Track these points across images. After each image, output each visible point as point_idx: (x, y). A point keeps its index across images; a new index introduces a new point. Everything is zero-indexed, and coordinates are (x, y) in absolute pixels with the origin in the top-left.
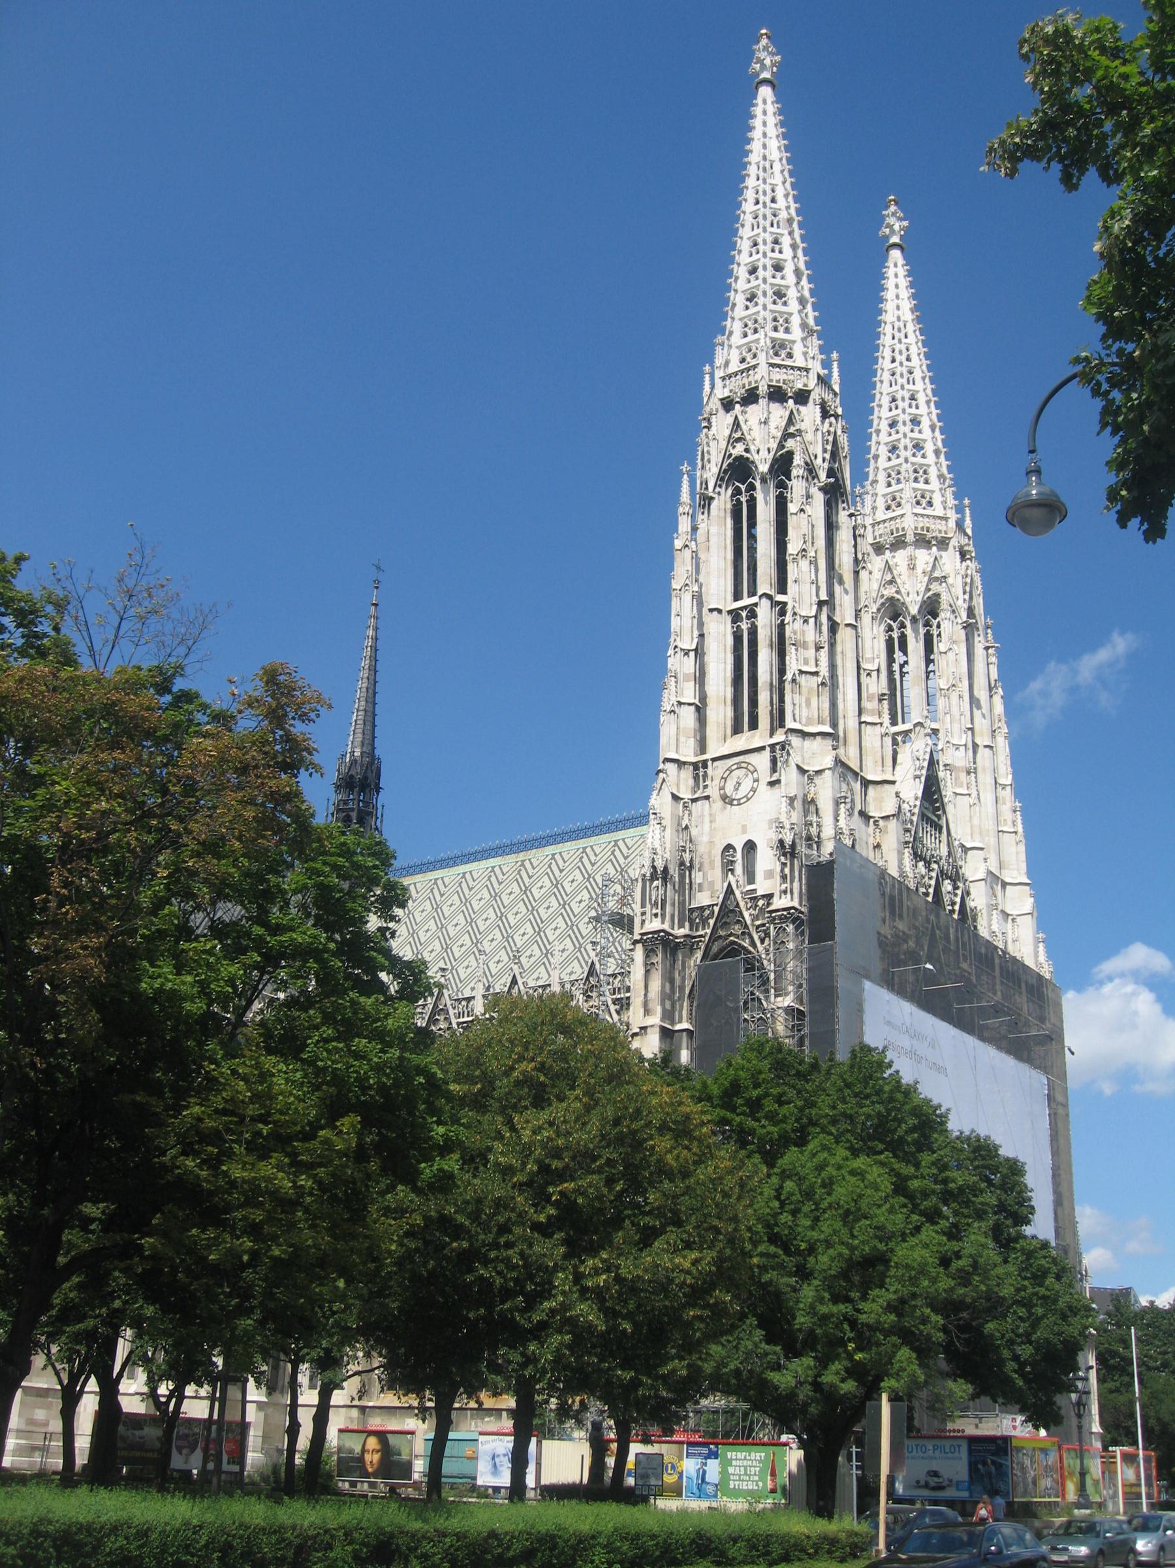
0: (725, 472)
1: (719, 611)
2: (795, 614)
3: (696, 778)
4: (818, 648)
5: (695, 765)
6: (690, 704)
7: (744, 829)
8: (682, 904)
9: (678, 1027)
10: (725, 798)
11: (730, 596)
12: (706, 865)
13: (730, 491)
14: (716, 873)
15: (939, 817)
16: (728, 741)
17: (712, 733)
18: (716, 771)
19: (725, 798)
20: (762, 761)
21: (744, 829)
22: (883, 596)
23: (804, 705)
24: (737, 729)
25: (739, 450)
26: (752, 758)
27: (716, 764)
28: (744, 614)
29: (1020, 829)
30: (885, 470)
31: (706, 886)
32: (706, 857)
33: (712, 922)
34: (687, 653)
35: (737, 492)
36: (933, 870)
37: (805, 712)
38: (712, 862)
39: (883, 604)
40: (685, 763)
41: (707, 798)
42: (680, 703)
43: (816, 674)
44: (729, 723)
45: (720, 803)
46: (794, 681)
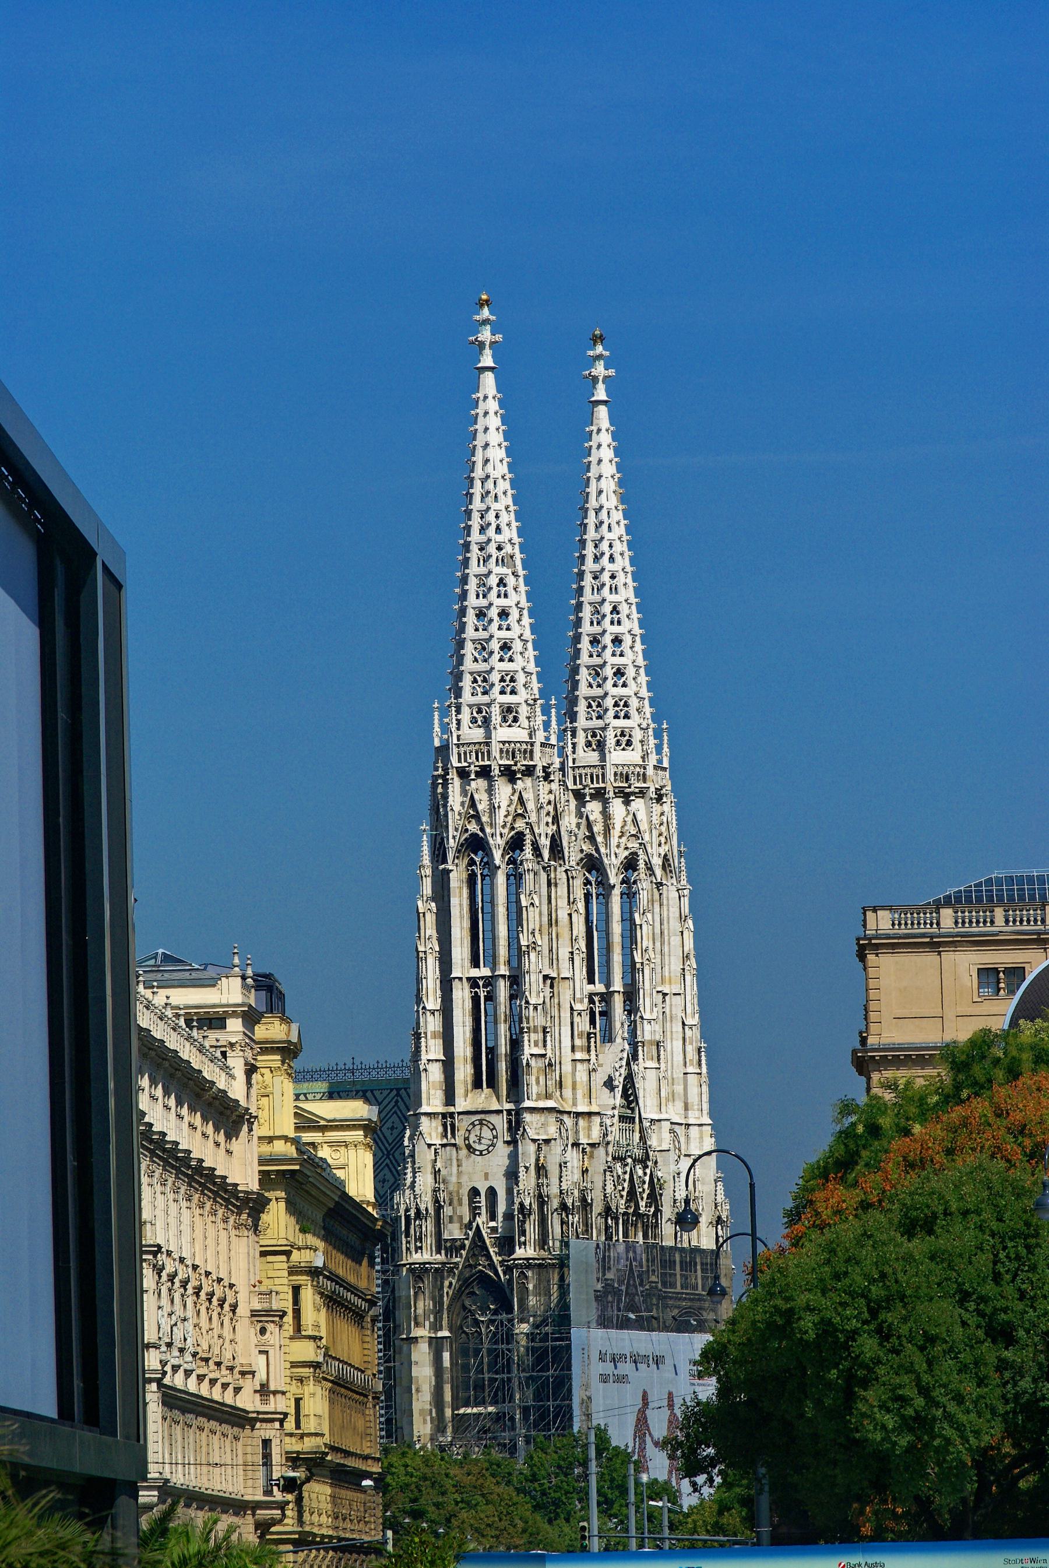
0: (462, 845)
1: (460, 979)
2: (527, 1002)
3: (445, 1126)
4: (545, 1032)
5: (444, 1116)
6: (437, 1060)
7: (486, 1179)
8: (438, 1234)
9: (440, 1334)
10: (469, 1147)
11: (467, 963)
12: (455, 1202)
13: (466, 861)
14: (465, 1212)
15: (633, 1109)
16: (469, 1095)
17: (459, 1090)
18: (463, 1124)
19: (469, 1147)
20: (500, 1123)
21: (486, 1179)
22: (582, 851)
23: (534, 1083)
24: (477, 1084)
25: (473, 827)
26: (494, 1119)
27: (461, 1117)
28: (481, 983)
29: (704, 1070)
30: (586, 698)
31: (455, 1218)
32: (455, 1194)
33: (464, 1253)
34: (433, 1012)
35: (472, 862)
36: (627, 1165)
37: (535, 1090)
38: (460, 1201)
39: (582, 859)
40: (434, 1114)
41: (454, 1145)
42: (429, 1060)
43: (544, 1056)
44: (469, 1079)
45: (464, 1152)
46: (528, 1064)
